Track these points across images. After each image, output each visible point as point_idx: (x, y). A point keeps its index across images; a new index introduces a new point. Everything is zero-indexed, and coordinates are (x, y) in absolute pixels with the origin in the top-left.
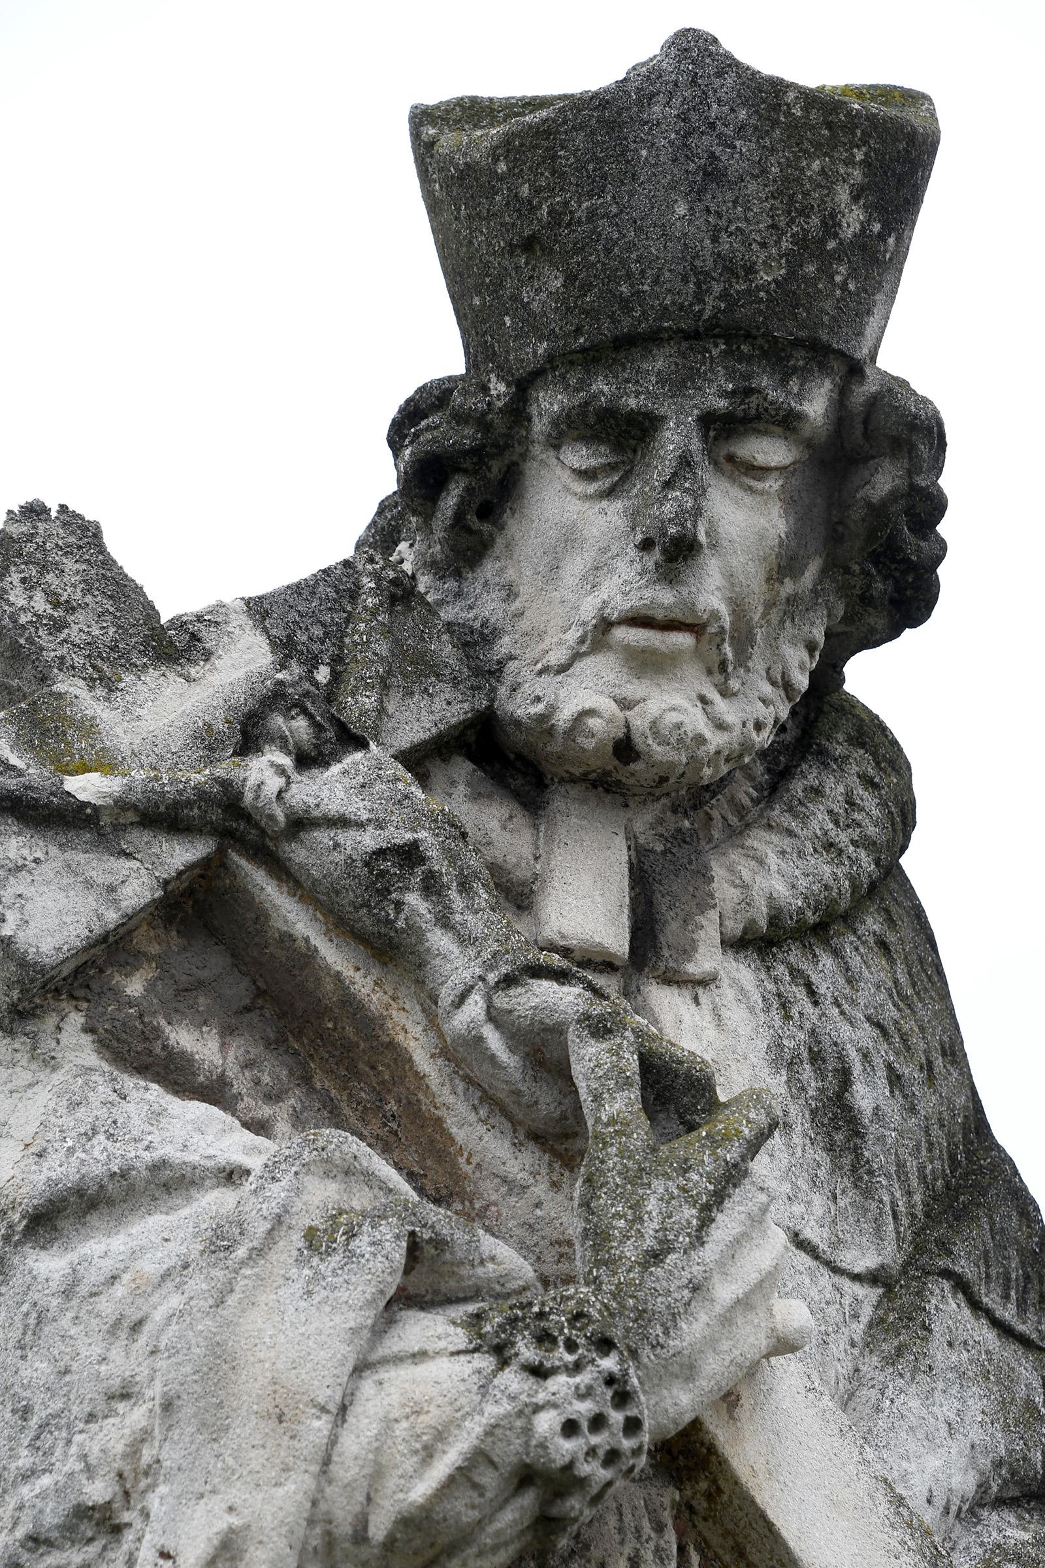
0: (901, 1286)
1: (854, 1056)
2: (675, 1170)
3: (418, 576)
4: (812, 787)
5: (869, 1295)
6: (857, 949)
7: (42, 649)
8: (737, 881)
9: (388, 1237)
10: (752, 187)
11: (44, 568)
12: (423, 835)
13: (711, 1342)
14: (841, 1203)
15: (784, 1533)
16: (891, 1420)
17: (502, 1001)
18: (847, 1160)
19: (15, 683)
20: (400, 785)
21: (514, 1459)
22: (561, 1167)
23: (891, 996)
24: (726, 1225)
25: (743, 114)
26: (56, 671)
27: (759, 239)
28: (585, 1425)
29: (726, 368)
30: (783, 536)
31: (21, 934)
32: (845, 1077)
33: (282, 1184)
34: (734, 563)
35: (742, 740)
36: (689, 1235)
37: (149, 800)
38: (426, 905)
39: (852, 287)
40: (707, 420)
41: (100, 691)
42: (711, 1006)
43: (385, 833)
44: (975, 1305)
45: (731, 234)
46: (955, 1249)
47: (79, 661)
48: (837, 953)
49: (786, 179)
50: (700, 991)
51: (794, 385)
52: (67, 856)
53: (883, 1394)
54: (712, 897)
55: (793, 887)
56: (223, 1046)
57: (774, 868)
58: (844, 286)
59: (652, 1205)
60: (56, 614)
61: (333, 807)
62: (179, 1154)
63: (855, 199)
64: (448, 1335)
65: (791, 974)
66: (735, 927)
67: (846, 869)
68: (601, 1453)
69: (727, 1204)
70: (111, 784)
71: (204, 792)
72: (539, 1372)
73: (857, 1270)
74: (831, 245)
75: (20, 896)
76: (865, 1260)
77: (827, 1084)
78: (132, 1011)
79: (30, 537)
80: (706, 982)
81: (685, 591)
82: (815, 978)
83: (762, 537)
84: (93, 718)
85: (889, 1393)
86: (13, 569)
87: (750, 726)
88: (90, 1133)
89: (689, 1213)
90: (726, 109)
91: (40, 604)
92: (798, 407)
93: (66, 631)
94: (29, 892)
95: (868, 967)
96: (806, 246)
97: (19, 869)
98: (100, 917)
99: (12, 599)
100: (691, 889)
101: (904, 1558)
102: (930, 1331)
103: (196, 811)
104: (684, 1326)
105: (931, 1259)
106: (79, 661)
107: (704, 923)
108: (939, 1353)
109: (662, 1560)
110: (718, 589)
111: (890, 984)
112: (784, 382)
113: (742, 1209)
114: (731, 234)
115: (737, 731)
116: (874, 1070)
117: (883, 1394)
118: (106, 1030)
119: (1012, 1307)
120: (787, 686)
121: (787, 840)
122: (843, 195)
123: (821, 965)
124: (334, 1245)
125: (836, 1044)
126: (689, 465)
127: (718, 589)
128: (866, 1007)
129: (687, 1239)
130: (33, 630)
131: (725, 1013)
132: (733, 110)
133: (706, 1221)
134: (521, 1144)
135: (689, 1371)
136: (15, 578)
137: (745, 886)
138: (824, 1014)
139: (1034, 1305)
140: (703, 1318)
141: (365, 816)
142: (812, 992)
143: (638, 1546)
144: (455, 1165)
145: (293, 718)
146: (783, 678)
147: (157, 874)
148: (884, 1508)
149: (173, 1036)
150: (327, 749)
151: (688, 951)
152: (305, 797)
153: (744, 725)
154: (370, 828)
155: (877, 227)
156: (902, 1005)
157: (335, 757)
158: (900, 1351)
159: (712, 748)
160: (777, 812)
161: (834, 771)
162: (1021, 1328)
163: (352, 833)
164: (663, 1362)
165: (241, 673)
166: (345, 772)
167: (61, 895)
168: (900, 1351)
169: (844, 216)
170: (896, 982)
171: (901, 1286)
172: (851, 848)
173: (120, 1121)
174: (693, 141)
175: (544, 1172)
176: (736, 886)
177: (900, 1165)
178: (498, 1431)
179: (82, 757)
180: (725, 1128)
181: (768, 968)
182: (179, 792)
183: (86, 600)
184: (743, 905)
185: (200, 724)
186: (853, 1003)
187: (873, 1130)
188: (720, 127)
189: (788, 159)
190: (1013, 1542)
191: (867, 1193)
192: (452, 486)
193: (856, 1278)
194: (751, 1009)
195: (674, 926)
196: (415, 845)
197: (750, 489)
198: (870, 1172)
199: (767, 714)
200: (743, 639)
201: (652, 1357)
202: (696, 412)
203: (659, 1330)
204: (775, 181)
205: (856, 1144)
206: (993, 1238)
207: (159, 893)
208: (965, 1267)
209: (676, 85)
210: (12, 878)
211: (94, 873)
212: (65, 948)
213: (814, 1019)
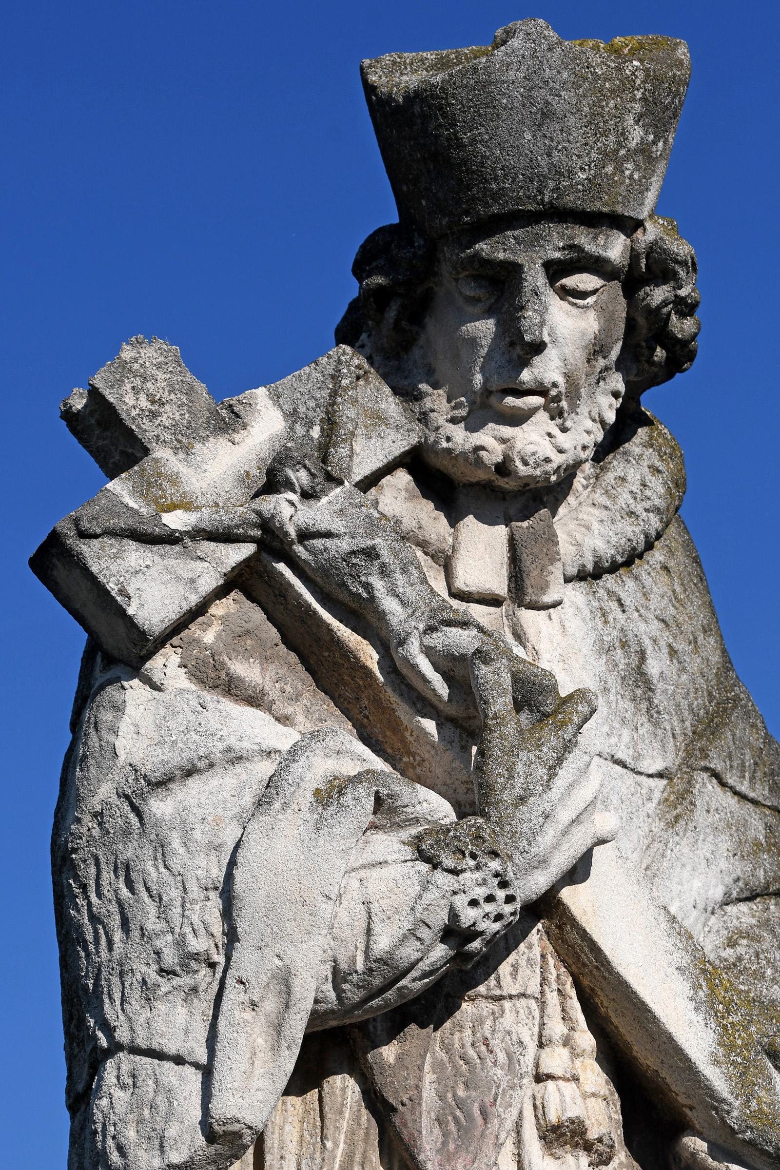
0: (678, 778)
1: (647, 643)
2: (532, 746)
3: (374, 356)
4: (620, 477)
5: (660, 784)
6: (649, 574)
7: (146, 431)
8: (574, 542)
9: (363, 794)
11: (145, 380)
12: (377, 541)
13: (556, 846)
14: (641, 732)
15: (603, 948)
16: (671, 862)
17: (428, 641)
18: (644, 706)
19: (130, 451)
20: (364, 509)
21: (441, 923)
22: (467, 736)
23: (671, 601)
24: (564, 775)
25: (565, 75)
26: (154, 444)
27: (577, 153)
28: (481, 901)
29: (558, 233)
30: (597, 332)
31: (140, 613)
32: (642, 656)
33: (299, 763)
34: (567, 352)
35: (574, 457)
36: (542, 785)
37: (213, 526)
38: (381, 583)
39: (636, 176)
40: (548, 266)
41: (181, 455)
42: (559, 620)
43: (355, 541)
44: (723, 784)
45: (560, 150)
46: (711, 754)
47: (168, 437)
48: (636, 578)
50: (551, 610)
51: (601, 240)
52: (166, 562)
53: (666, 846)
54: (558, 554)
55: (608, 542)
56: (263, 670)
57: (596, 532)
58: (631, 177)
59: (520, 768)
60: (153, 408)
61: (323, 526)
62: (238, 743)
63: (637, 122)
64: (400, 850)
65: (608, 594)
66: (573, 571)
67: (641, 528)
68: (492, 916)
69: (565, 764)
70: (190, 517)
71: (247, 519)
72: (455, 872)
73: (650, 772)
74: (622, 152)
75: (138, 589)
76: (657, 766)
77: (631, 661)
78: (207, 653)
79: (136, 360)
80: (555, 605)
81: (536, 371)
82: (623, 596)
83: (584, 334)
84: (178, 473)
85: (670, 845)
86: (126, 381)
87: (579, 448)
88: (186, 731)
89: (542, 772)
90: (554, 72)
91: (144, 402)
92: (604, 254)
93: (160, 419)
94: (144, 586)
95: (656, 584)
96: (607, 155)
97: (137, 572)
98: (186, 599)
99: (127, 400)
100: (545, 550)
101: (676, 955)
102: (695, 806)
103: (241, 530)
104: (540, 839)
105: (696, 760)
106: (168, 437)
107: (554, 570)
108: (700, 817)
109: (531, 965)
110: (557, 368)
111: (670, 593)
112: (595, 238)
113: (574, 766)
114: (560, 150)
115: (572, 452)
116: (660, 649)
117: (666, 846)
118: (193, 665)
119: (746, 783)
120: (603, 422)
121: (605, 513)
122: (630, 120)
123: (627, 586)
124: (331, 800)
125: (636, 636)
126: (537, 295)
127: (557, 368)
128: (655, 610)
129: (541, 788)
130: (139, 420)
131: (567, 624)
132: (559, 72)
133: (552, 776)
134: (442, 724)
135: (542, 862)
136: (128, 387)
137: (578, 544)
138: (629, 618)
139: (760, 780)
140: (551, 833)
141: (343, 530)
142: (621, 605)
143: (517, 958)
144: (403, 736)
145: (298, 471)
146: (599, 417)
147: (219, 570)
148: (664, 925)
149: (232, 667)
150: (318, 488)
151: (544, 588)
152: (307, 520)
154: (346, 538)
155: (651, 137)
156: (678, 605)
157: (324, 492)
158: (677, 818)
159: (555, 465)
160: (598, 495)
161: (633, 465)
162: (752, 795)
163: (336, 541)
164: (528, 861)
165: (265, 436)
166: (330, 502)
167: (162, 587)
168: (677, 818)
169: (630, 133)
170: (674, 591)
171: (678, 778)
172: (645, 514)
173: (203, 723)
174: (535, 93)
175: (457, 740)
176: (573, 545)
177: (678, 705)
178: (430, 908)
179: (172, 499)
180: (564, 718)
181: (594, 592)
182: (232, 520)
183: (171, 398)
184: (578, 557)
185: (242, 472)
186: (647, 608)
187: (660, 686)
188: (551, 84)
189: (594, 101)
190: (745, 925)
191: (656, 724)
192: (392, 304)
193: (650, 776)
194: (584, 620)
195: (535, 573)
196: (373, 548)
198: (658, 712)
199: (589, 440)
200: (573, 392)
201: (521, 859)
202: (541, 261)
203: (525, 843)
204: (586, 116)
206: (734, 743)
207: (221, 582)
208: (716, 764)
209: (523, 57)
210: (133, 578)
211: (182, 572)
212: (166, 620)
213: (622, 622)
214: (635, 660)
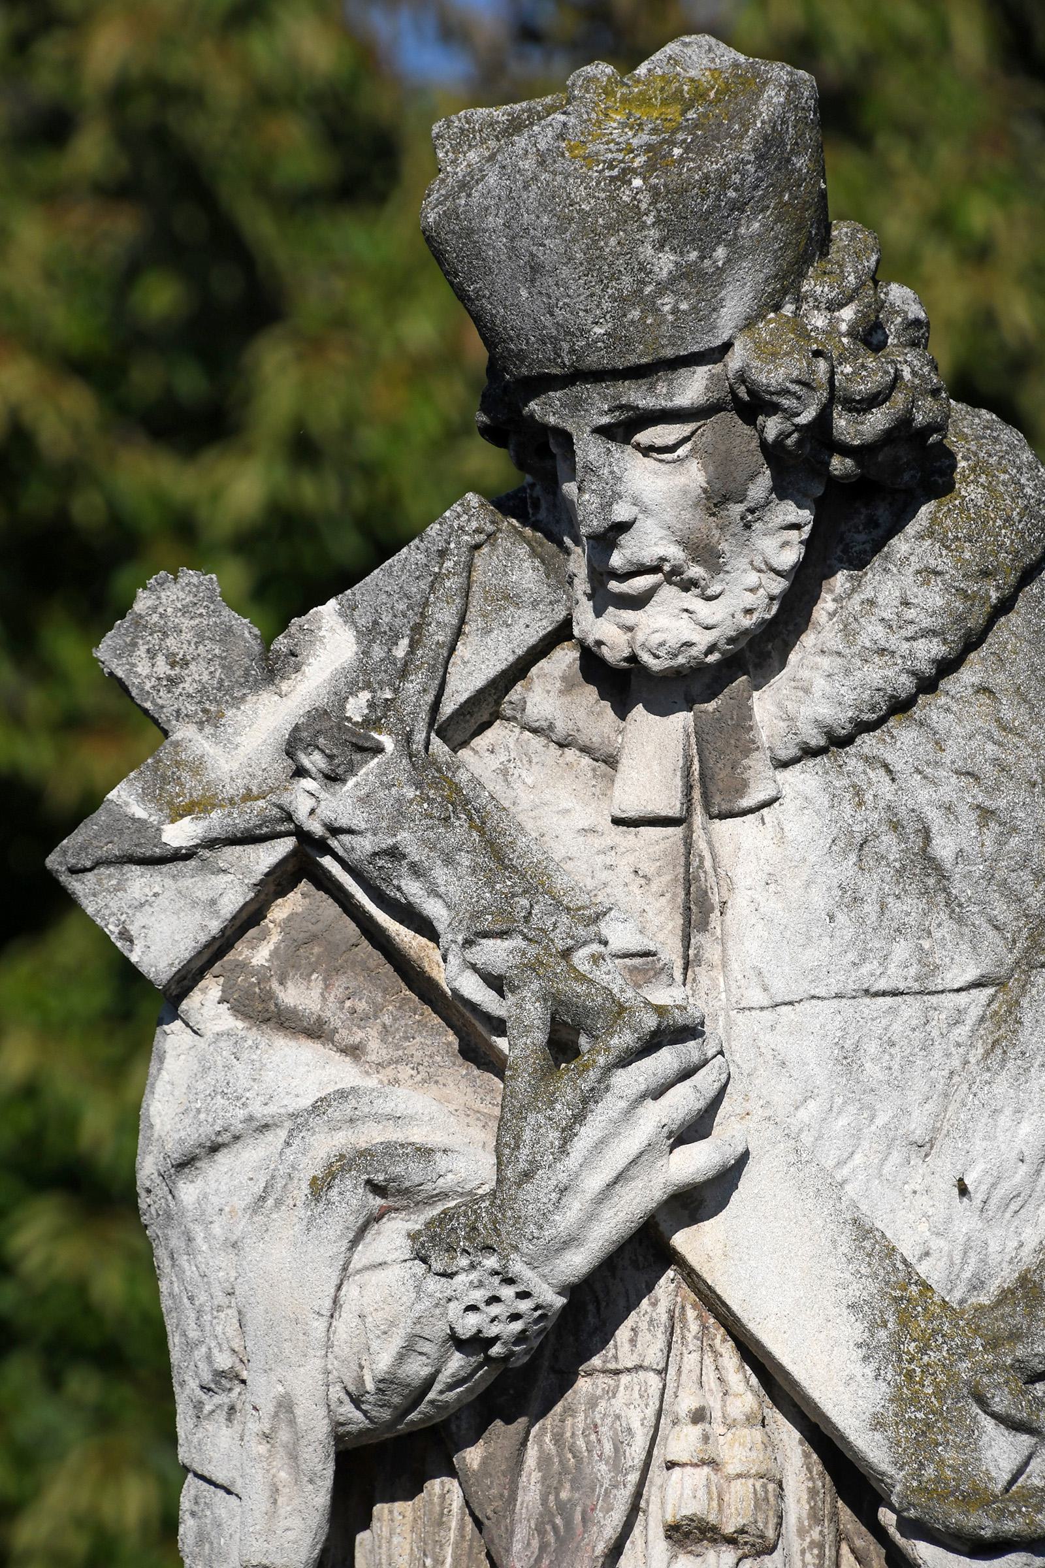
8: (784, 716)
10: (565, 272)
32: (926, 834)
34: (667, 518)
49: (590, 261)
75: (144, 927)
82: (890, 758)
83: (685, 493)
87: (740, 616)
100: (733, 742)
114: (561, 309)
116: (957, 818)
122: (648, 251)
147: (246, 881)
151: (742, 788)
153: (733, 616)
176: (784, 720)
197: (661, 461)
204: (581, 264)
205: (944, 885)
214: (916, 842)
